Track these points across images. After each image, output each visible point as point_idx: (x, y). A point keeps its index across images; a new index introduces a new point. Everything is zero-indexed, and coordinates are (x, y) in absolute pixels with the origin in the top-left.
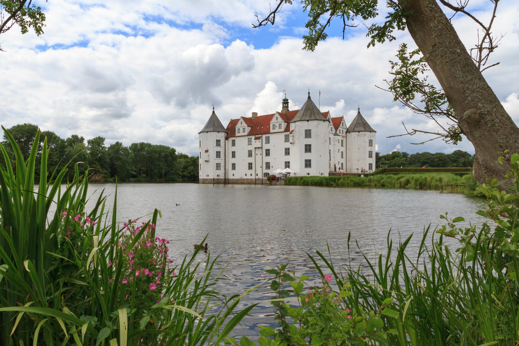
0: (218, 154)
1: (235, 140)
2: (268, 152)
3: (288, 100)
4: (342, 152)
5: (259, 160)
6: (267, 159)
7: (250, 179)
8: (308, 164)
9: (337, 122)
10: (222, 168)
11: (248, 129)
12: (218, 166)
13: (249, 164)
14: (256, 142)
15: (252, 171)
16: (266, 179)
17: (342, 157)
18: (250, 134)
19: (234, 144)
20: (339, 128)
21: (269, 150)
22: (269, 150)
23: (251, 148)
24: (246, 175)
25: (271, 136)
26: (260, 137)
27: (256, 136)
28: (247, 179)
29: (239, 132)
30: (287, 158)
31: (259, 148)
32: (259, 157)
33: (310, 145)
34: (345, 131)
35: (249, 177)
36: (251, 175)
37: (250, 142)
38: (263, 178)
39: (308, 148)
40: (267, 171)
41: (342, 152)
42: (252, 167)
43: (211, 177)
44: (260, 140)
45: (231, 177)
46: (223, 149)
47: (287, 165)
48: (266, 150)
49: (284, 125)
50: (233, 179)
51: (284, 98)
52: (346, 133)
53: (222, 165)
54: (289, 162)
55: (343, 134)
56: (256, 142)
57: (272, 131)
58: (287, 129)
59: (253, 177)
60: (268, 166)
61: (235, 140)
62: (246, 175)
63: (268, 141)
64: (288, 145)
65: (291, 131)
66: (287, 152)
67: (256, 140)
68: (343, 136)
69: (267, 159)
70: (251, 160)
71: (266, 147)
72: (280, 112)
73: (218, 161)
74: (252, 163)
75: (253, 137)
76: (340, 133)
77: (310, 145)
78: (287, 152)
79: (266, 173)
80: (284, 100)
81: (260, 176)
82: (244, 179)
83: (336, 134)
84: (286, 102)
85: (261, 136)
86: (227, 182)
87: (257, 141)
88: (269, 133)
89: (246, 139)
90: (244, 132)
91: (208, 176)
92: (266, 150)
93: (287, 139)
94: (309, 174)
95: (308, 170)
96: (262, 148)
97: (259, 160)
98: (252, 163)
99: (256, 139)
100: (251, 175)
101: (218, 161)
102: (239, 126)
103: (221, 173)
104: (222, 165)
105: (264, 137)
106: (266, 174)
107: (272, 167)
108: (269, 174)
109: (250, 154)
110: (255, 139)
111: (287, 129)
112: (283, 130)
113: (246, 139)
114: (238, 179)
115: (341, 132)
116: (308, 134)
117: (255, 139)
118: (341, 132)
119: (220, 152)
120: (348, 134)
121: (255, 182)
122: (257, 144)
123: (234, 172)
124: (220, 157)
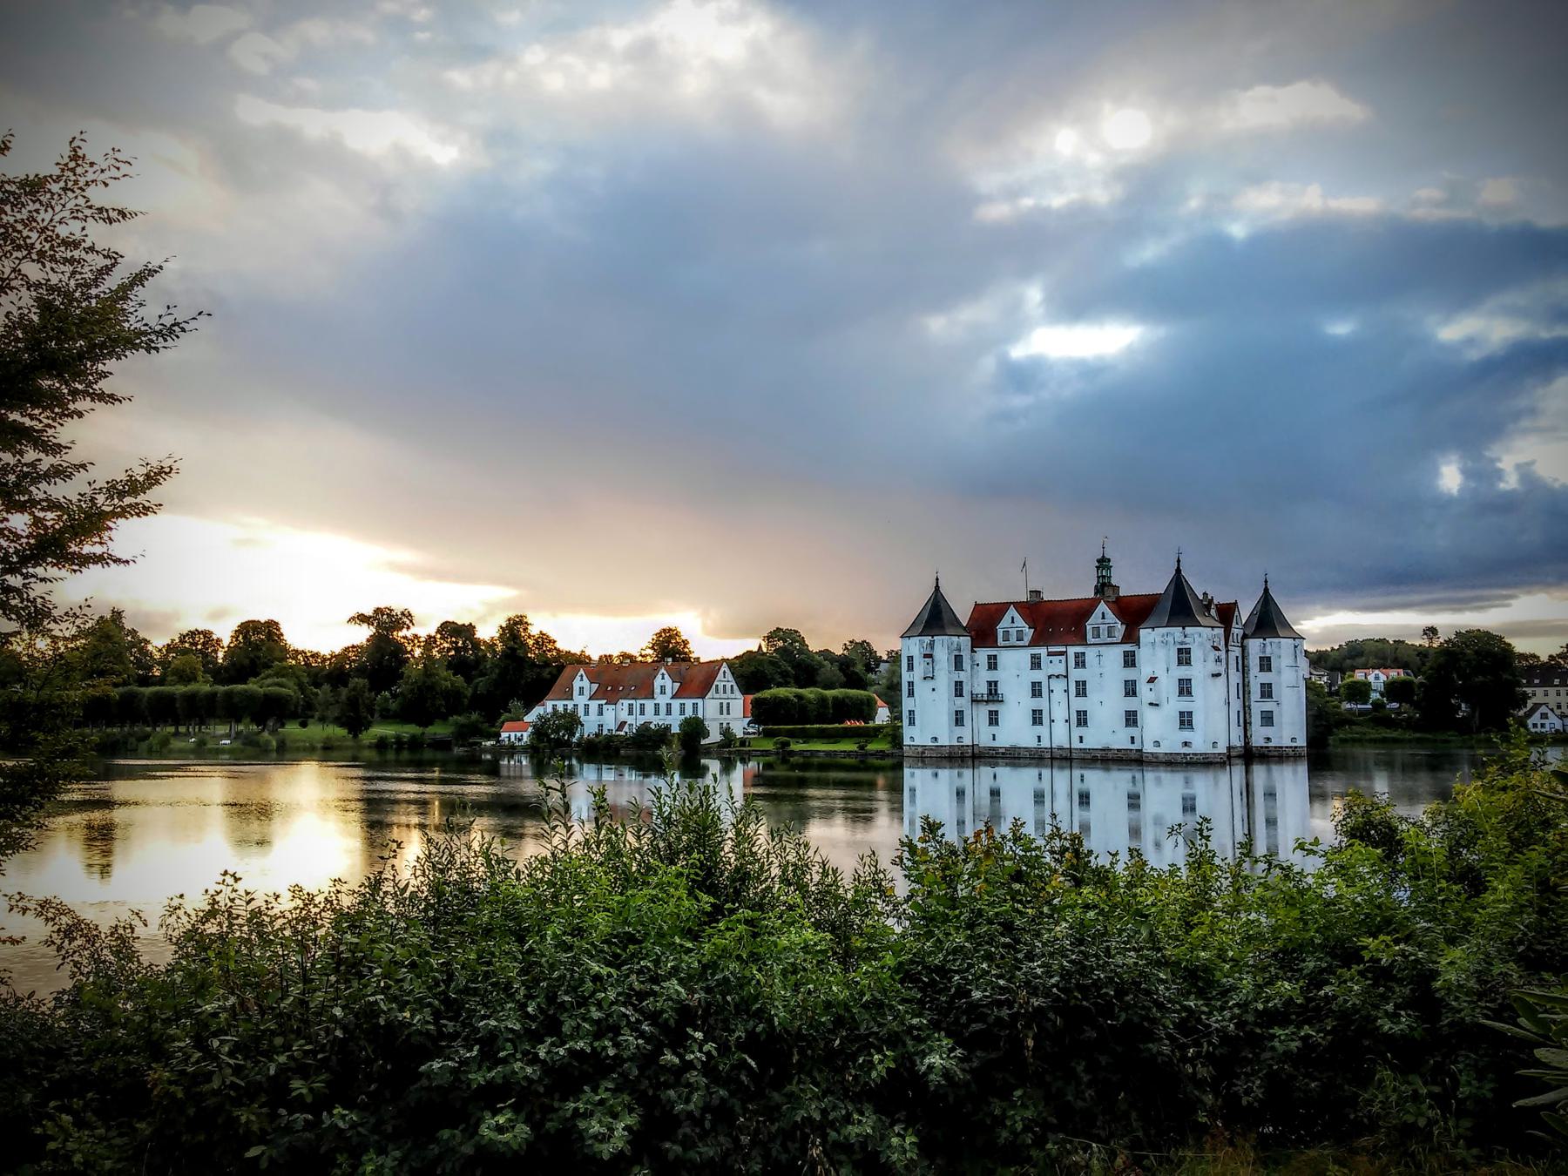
1: (995, 656)
5: (1059, 706)
6: (1079, 704)
8: (1186, 720)
9: (1226, 614)
11: (1029, 633)
15: (1043, 730)
18: (1034, 643)
19: (993, 664)
21: (1084, 683)
22: (1084, 683)
23: (1038, 676)
25: (1090, 653)
26: (1061, 653)
27: (1052, 649)
29: (1006, 639)
31: (1058, 677)
37: (1036, 663)
43: (944, 741)
44: (1063, 658)
45: (984, 741)
49: (1120, 628)
51: (1100, 557)
58: (1131, 637)
60: (1082, 718)
61: (995, 656)
63: (1080, 662)
67: (1051, 658)
69: (1079, 704)
71: (1076, 674)
75: (1042, 651)
80: (1098, 561)
84: (1103, 563)
85: (1063, 649)
86: (976, 751)
87: (1055, 659)
89: (1024, 656)
90: (1020, 639)
91: (936, 739)
93: (1130, 661)
94: (1186, 744)
95: (1186, 735)
96: (1066, 677)
97: (1059, 706)
102: (1005, 622)
105: (1072, 650)
109: (1036, 690)
113: (1024, 656)
120: (1245, 641)
123: (994, 729)
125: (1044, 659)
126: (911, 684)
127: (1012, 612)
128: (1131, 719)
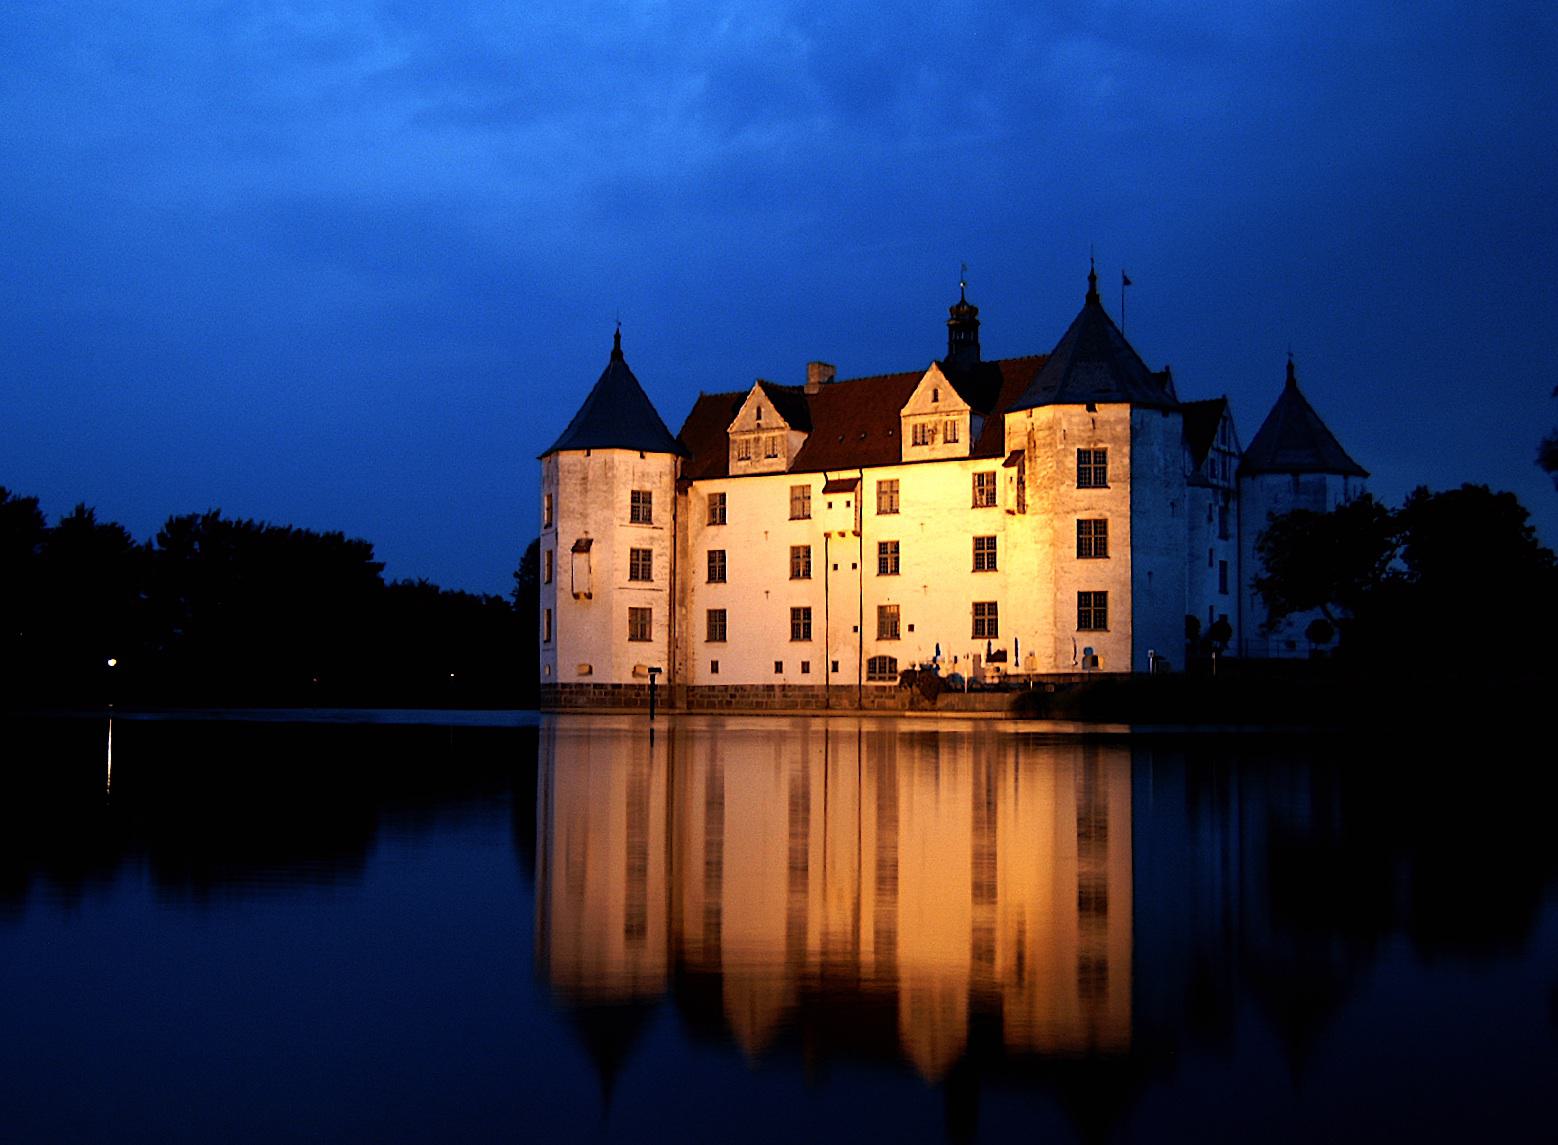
0: (640, 565)
1: (723, 496)
2: (889, 558)
3: (973, 311)
4: (1223, 565)
7: (801, 687)
8: (1091, 610)
10: (659, 633)
12: (640, 625)
13: (795, 612)
14: (830, 505)
16: (877, 687)
17: (1223, 590)
18: (802, 464)
19: (717, 512)
20: (1211, 454)
23: (802, 533)
24: (779, 667)
27: (833, 476)
28: (783, 687)
30: (984, 587)
32: (844, 583)
33: (1101, 525)
34: (1235, 463)
35: (793, 676)
36: (806, 667)
37: (800, 508)
38: (864, 682)
39: (1091, 540)
40: (887, 648)
41: (1223, 565)
42: (808, 627)
44: (850, 496)
46: (667, 533)
47: (985, 619)
48: (882, 546)
50: (712, 688)
52: (1239, 474)
53: (660, 615)
54: (993, 607)
55: (1224, 478)
56: (830, 505)
57: (909, 452)
59: (817, 678)
60: (889, 624)
62: (779, 667)
64: (986, 522)
65: (1007, 455)
66: (985, 554)
67: (831, 497)
68: (1227, 494)
70: (803, 594)
71: (879, 529)
72: (942, 361)
73: (639, 595)
74: (807, 611)
75: (817, 481)
76: (1213, 476)
77: (1101, 525)
78: (985, 554)
79: (883, 658)
81: (847, 676)
82: (770, 688)
83: (1196, 481)
85: (854, 474)
87: (840, 499)
88: (896, 460)
91: (590, 672)
92: (882, 546)
93: (985, 492)
96: (858, 534)
98: (807, 611)
99: (831, 488)
100: (806, 667)
101: (639, 595)
103: (653, 653)
104: (660, 615)
105: (872, 477)
106: (881, 666)
107: (911, 628)
108: (893, 661)
109: (800, 564)
110: (825, 491)
111: (987, 442)
112: (963, 448)
114: (736, 688)
115: (1219, 471)
116: (1091, 470)
117: (825, 491)
118: (1219, 471)
119: (648, 553)
120: (1247, 482)
121: (824, 700)
122: (832, 513)
123: (716, 651)
124: (647, 577)
125: (818, 500)
126: (550, 553)
127: (757, 395)
128: (985, 619)
